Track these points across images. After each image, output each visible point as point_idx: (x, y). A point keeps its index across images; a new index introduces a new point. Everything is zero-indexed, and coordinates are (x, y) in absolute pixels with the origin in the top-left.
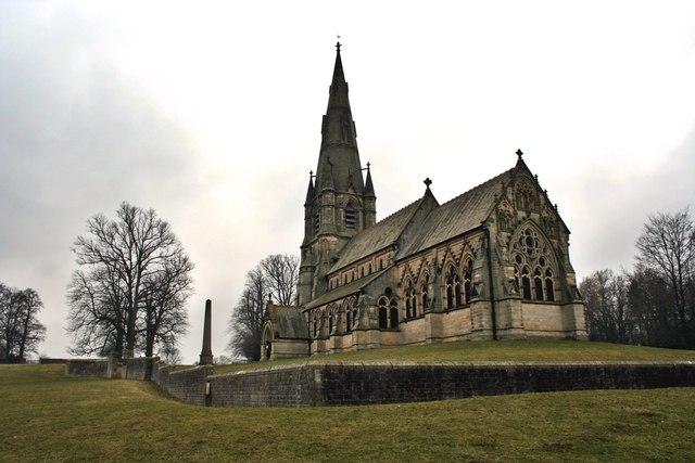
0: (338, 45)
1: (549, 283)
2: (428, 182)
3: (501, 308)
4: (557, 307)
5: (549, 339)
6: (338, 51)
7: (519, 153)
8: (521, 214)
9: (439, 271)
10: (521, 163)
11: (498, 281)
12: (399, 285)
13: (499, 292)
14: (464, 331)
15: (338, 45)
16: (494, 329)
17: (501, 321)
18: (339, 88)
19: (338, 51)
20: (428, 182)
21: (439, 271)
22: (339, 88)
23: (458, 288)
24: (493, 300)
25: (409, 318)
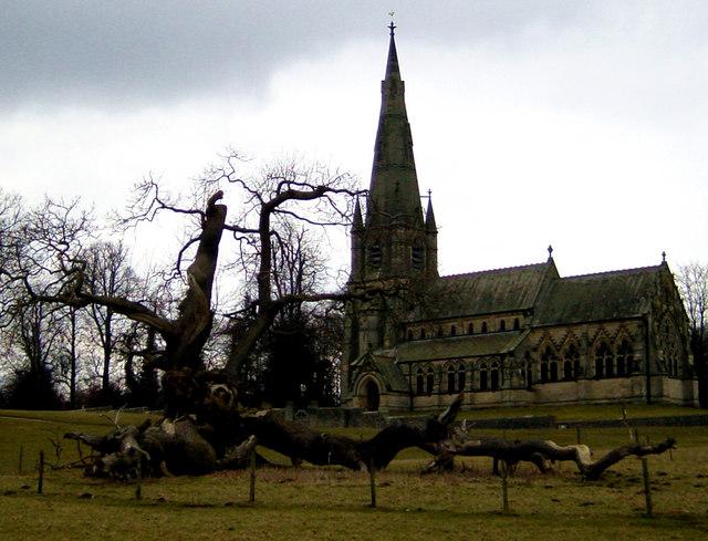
0: (392, 28)
1: (676, 361)
2: (550, 250)
3: (654, 381)
4: (679, 381)
5: (677, 405)
6: (392, 34)
7: (664, 255)
8: (665, 307)
9: (590, 344)
10: (664, 264)
11: (652, 361)
12: (535, 350)
13: (654, 369)
14: (616, 396)
15: (392, 28)
16: (649, 395)
17: (654, 391)
18: (393, 88)
19: (392, 34)
20: (550, 250)
21: (590, 344)
22: (393, 88)
23: (609, 361)
24: (649, 375)
25: (544, 380)
